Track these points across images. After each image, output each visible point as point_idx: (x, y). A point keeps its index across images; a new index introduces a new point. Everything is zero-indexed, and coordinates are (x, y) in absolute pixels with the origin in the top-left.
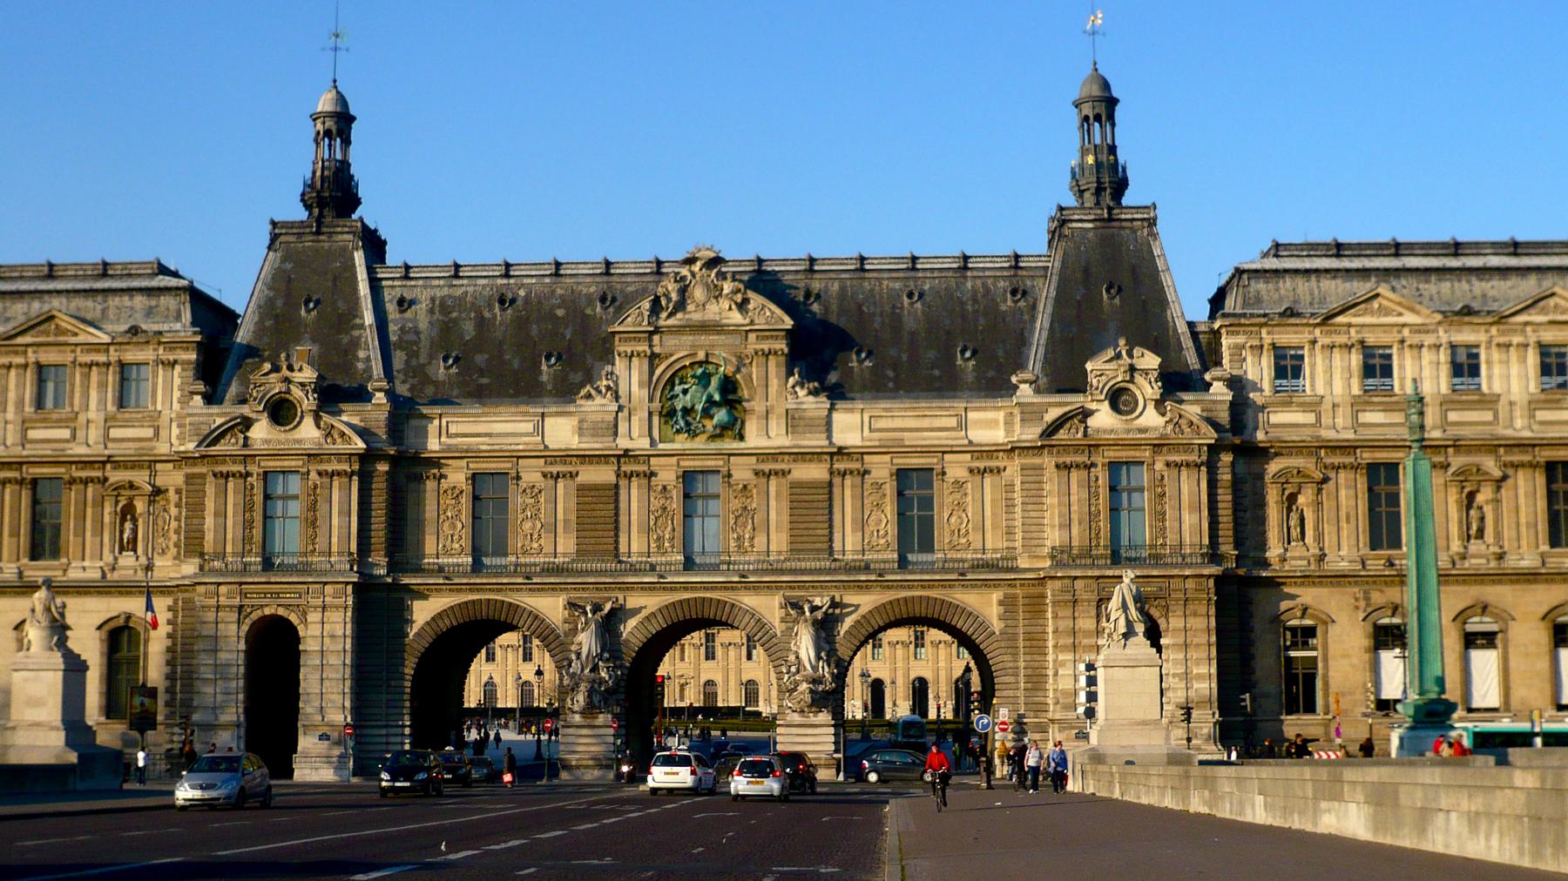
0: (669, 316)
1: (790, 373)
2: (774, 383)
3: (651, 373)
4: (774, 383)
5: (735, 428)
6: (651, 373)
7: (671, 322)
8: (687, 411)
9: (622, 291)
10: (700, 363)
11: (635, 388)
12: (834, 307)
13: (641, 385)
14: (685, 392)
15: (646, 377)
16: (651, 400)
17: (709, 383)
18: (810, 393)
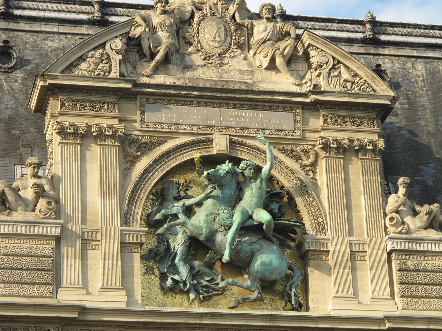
0: (156, 70)
1: (389, 188)
2: (362, 203)
3: (125, 173)
4: (362, 203)
5: (286, 287)
6: (125, 173)
7: (160, 79)
8: (198, 246)
9: (35, 47)
10: (218, 160)
11: (94, 198)
12: (424, 100)
13: (104, 191)
14: (189, 211)
15: (114, 174)
16: (126, 219)
17: (239, 198)
18: (432, 224)
